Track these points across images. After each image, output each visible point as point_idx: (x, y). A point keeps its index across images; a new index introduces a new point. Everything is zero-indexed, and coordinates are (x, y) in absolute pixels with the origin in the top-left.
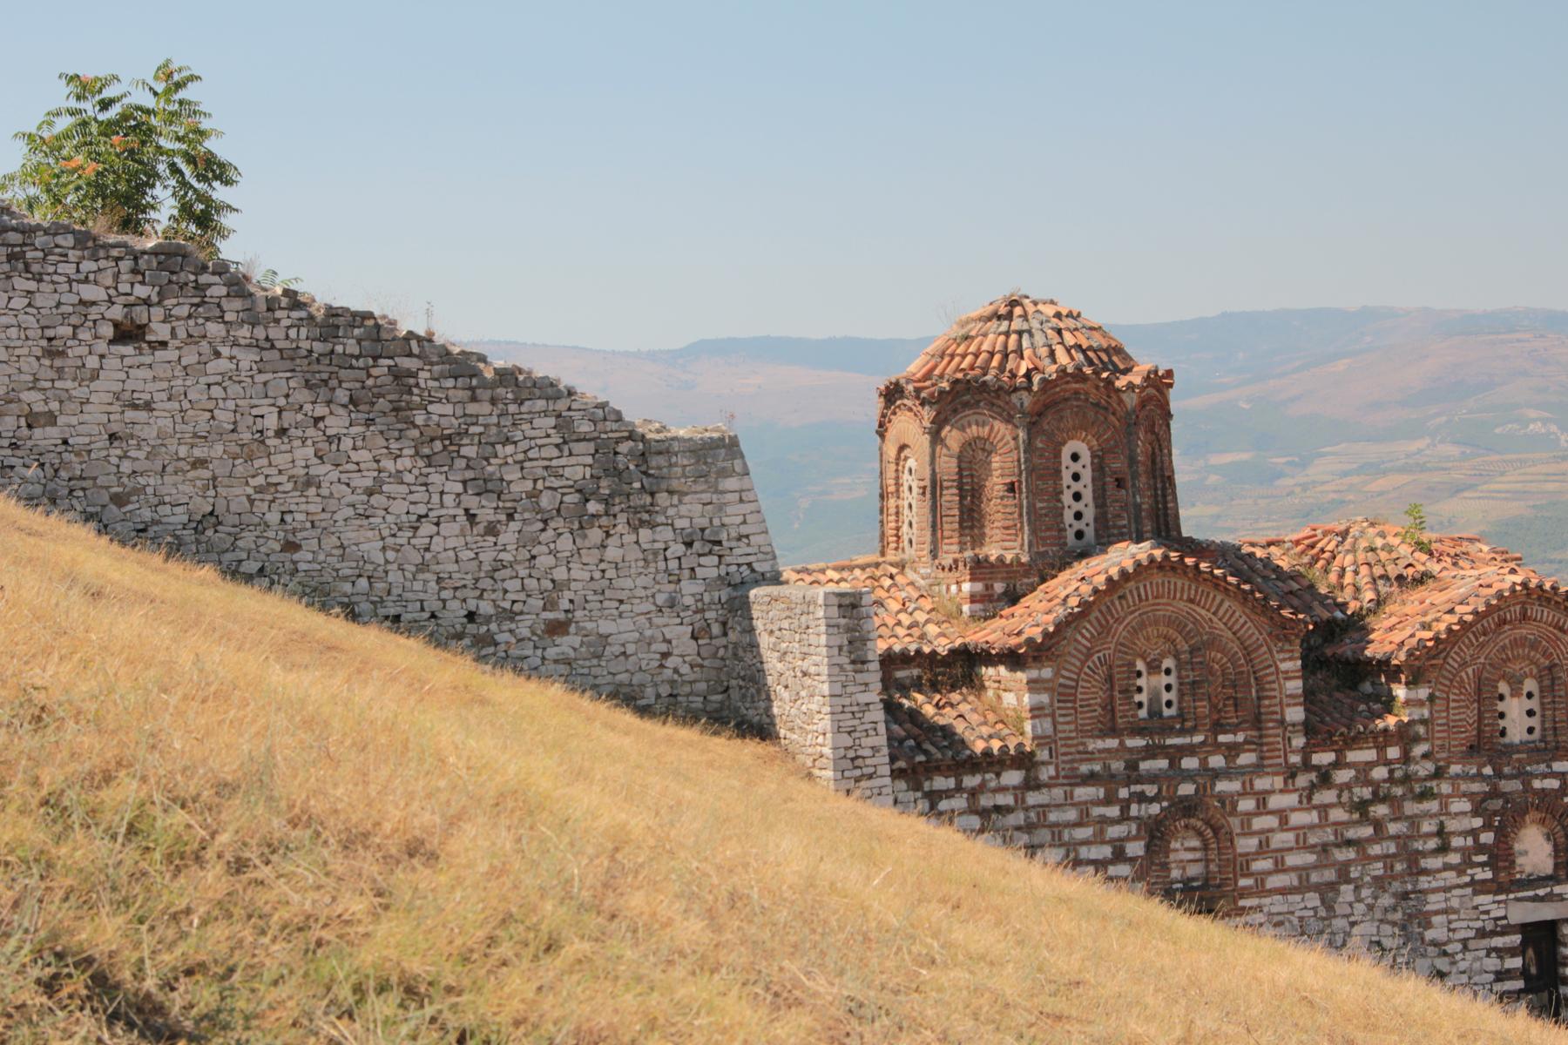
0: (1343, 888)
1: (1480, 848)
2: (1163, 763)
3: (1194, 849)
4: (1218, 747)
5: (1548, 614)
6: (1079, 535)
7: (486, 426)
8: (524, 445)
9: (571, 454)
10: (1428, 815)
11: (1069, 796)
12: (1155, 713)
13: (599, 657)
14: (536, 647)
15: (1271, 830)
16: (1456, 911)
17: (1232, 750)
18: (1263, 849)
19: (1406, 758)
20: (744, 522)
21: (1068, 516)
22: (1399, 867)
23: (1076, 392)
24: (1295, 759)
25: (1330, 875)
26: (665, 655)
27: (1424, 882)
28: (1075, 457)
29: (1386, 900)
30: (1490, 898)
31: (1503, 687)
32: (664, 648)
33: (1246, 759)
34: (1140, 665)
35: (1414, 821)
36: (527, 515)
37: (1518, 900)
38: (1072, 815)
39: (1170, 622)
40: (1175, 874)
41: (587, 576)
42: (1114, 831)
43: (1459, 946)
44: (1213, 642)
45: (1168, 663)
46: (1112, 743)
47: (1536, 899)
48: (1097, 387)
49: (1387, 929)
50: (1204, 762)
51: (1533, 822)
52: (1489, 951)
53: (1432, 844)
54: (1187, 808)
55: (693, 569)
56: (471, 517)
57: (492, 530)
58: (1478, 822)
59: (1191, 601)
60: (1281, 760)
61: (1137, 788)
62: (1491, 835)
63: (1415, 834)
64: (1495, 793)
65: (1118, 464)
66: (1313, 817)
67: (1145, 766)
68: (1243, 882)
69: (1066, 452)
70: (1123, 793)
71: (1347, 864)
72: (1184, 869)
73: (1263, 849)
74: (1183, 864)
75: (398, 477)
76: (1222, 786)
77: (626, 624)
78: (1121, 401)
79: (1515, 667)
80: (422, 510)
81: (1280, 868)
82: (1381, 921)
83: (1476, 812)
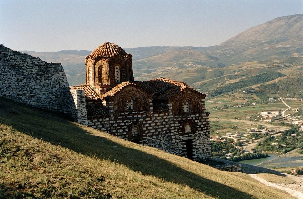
0: (159, 135)
1: (180, 128)
2: (131, 117)
3: (136, 130)
4: (140, 114)
5: (190, 92)
6: (118, 81)
7: (20, 63)
8: (26, 66)
9: (34, 68)
10: (172, 124)
12: (130, 109)
13: (40, 101)
14: (29, 100)
16: (177, 138)
17: (142, 114)
18: (147, 130)
19: (168, 115)
20: (63, 79)
21: (116, 78)
23: (117, 58)
25: (157, 133)
26: (51, 101)
27: (171, 134)
28: (117, 68)
29: (166, 137)
30: (181, 136)
31: (183, 104)
32: (50, 99)
33: (144, 115)
34: (127, 101)
35: (170, 125)
36: (27, 78)
38: (117, 125)
39: (132, 94)
40: (133, 134)
41: (37, 88)
42: (124, 127)
43: (177, 144)
44: (139, 98)
45: (132, 101)
47: (188, 136)
48: (120, 57)
49: (166, 141)
50: (137, 116)
52: (181, 144)
53: (173, 128)
54: (135, 123)
55: (55, 87)
56: (18, 79)
57: (21, 80)
58: (180, 124)
59: (135, 91)
60: (149, 116)
61: (127, 120)
62: (181, 126)
63: (170, 126)
65: (124, 69)
66: (155, 124)
67: (128, 117)
68: (144, 135)
69: (115, 67)
70: (125, 121)
71: (160, 131)
72: (134, 133)
73: (147, 130)
74: (134, 132)
75: (5, 72)
76: (140, 120)
77: (44, 95)
78: (124, 60)
79: (185, 101)
80: (9, 77)
81: (149, 132)
83: (179, 123)
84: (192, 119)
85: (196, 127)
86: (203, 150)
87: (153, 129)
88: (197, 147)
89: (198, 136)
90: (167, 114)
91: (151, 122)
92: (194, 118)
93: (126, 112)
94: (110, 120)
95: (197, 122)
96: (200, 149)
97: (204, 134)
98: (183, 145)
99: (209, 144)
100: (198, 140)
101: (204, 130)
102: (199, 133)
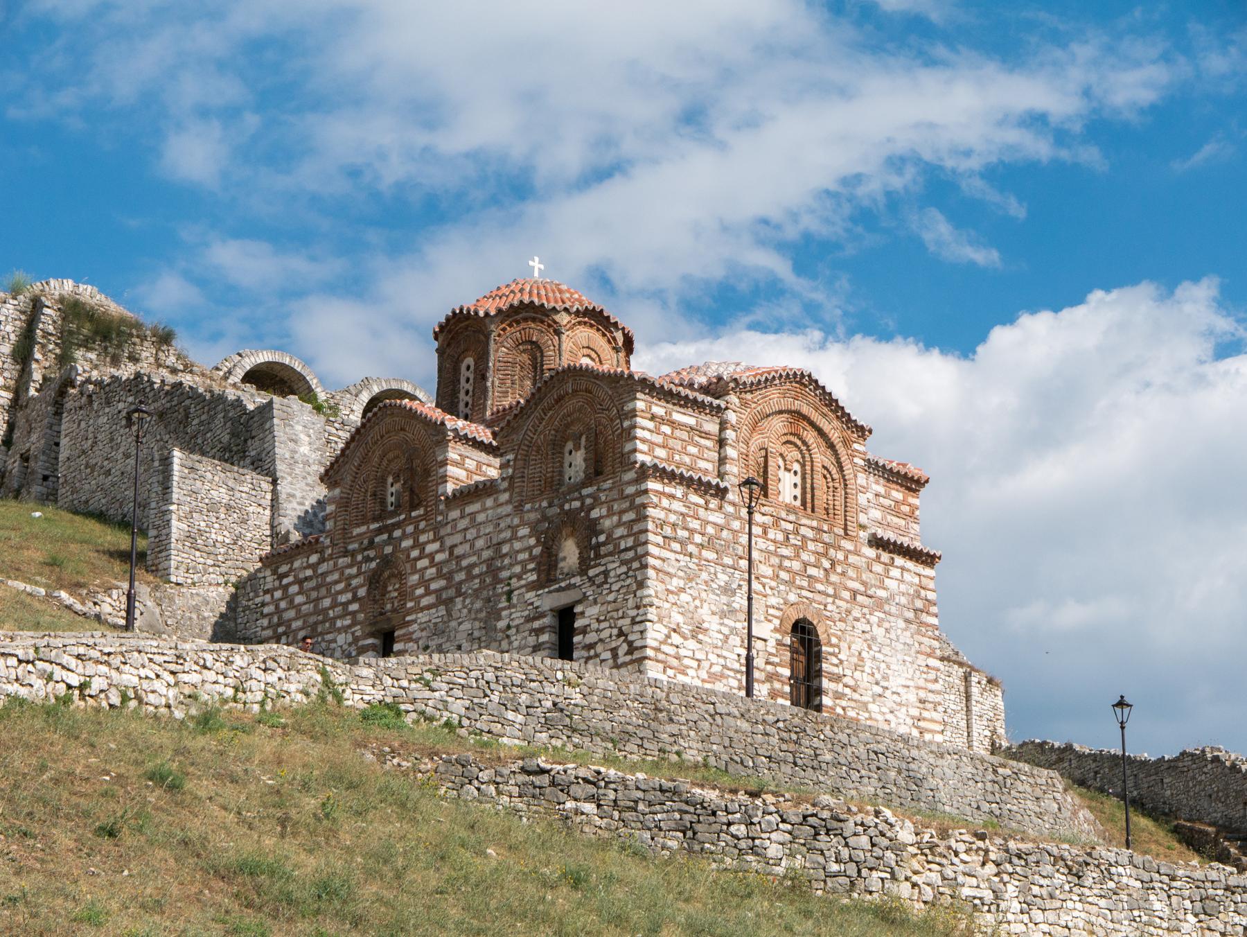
2: (385, 536)
10: (504, 542)
11: (335, 564)
15: (426, 568)
22: (488, 580)
24: (440, 518)
25: (452, 592)
28: (468, 368)
30: (532, 594)
37: (550, 592)
38: (336, 576)
46: (363, 529)
47: (560, 590)
49: (477, 624)
50: (404, 531)
51: (568, 536)
54: (386, 562)
64: (545, 518)
67: (377, 540)
68: (410, 605)
70: (359, 558)
71: (461, 583)
79: (576, 428)
81: (428, 592)
82: (475, 619)
84: (583, 504)
85: (594, 541)
86: (614, 651)
87: (440, 575)
88: (591, 638)
89: (598, 587)
90: (489, 502)
91: (436, 546)
92: (589, 501)
93: (375, 520)
94: (322, 560)
95: (601, 517)
96: (599, 648)
97: (624, 569)
98: (537, 636)
99: (638, 619)
100: (595, 602)
101: (627, 549)
102: (603, 568)
